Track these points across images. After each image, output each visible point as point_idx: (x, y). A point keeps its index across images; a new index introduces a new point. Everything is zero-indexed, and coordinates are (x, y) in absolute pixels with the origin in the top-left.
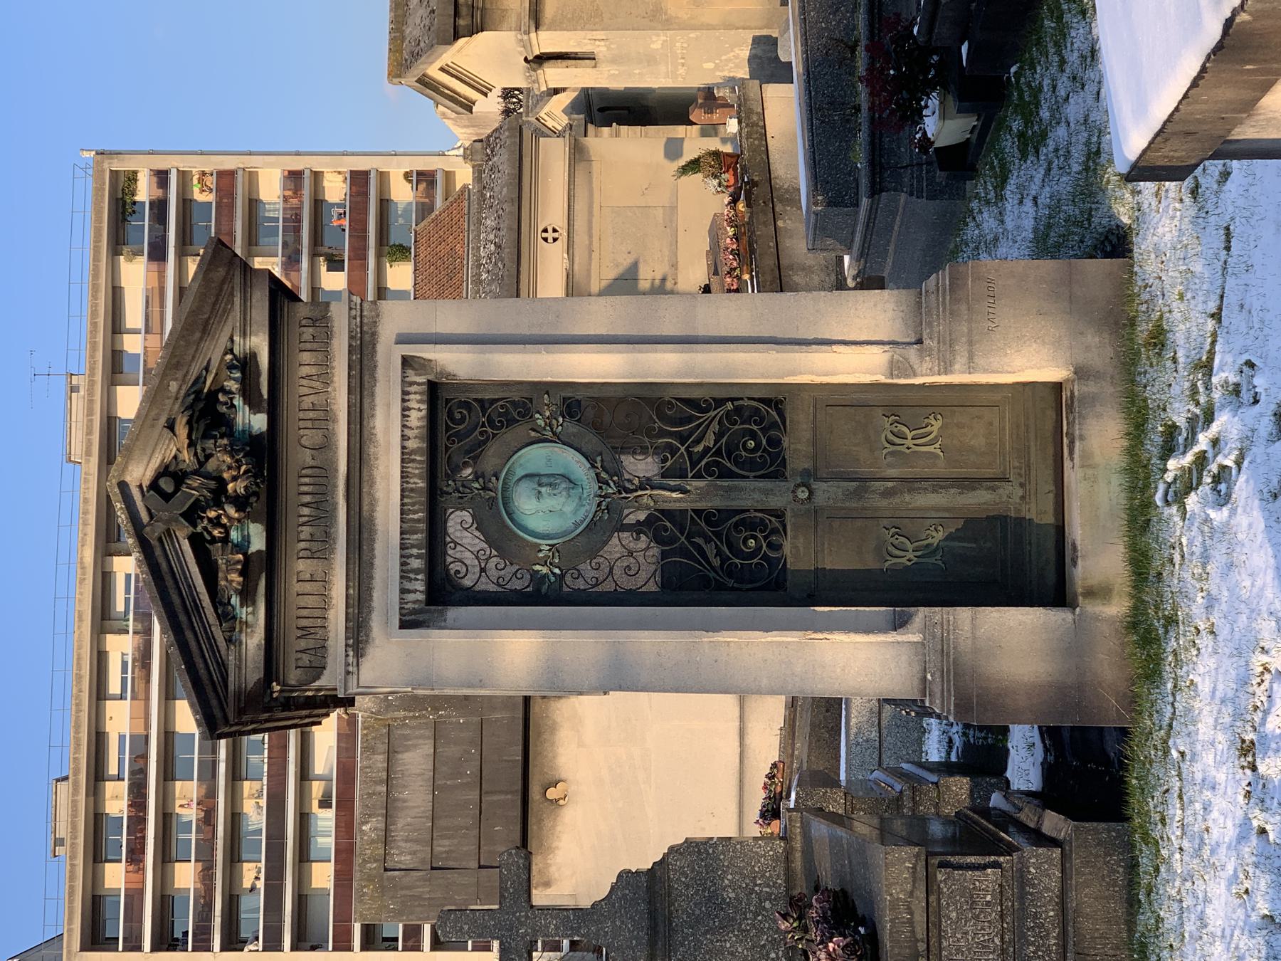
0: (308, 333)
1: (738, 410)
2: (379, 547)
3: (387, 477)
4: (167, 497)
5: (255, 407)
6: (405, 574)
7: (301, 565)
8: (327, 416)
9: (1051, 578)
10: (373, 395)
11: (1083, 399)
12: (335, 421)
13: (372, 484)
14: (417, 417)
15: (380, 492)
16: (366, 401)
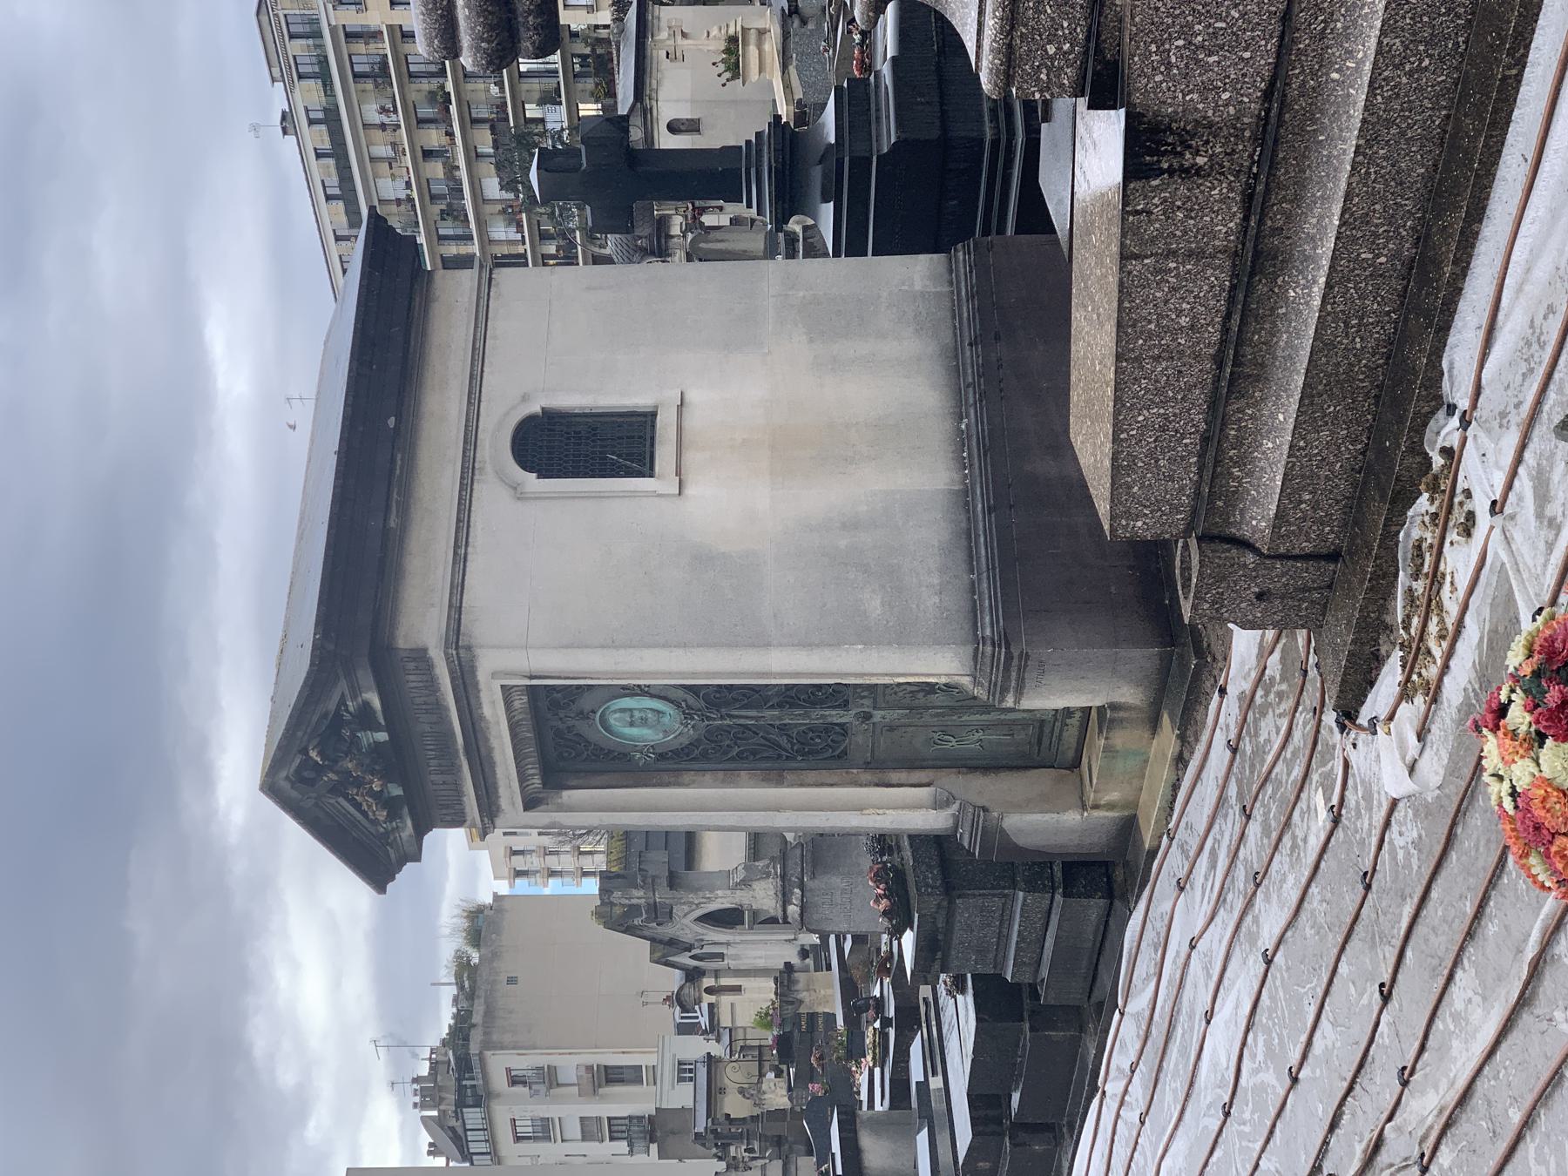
0: (411, 665)
1: (811, 729)
2: (500, 771)
3: (500, 737)
4: (310, 782)
5: (378, 729)
6: (523, 778)
7: (433, 777)
8: (439, 708)
9: (1071, 754)
10: (478, 697)
11: (1112, 721)
12: (447, 709)
13: (487, 740)
14: (520, 702)
15: (494, 743)
16: (473, 701)
